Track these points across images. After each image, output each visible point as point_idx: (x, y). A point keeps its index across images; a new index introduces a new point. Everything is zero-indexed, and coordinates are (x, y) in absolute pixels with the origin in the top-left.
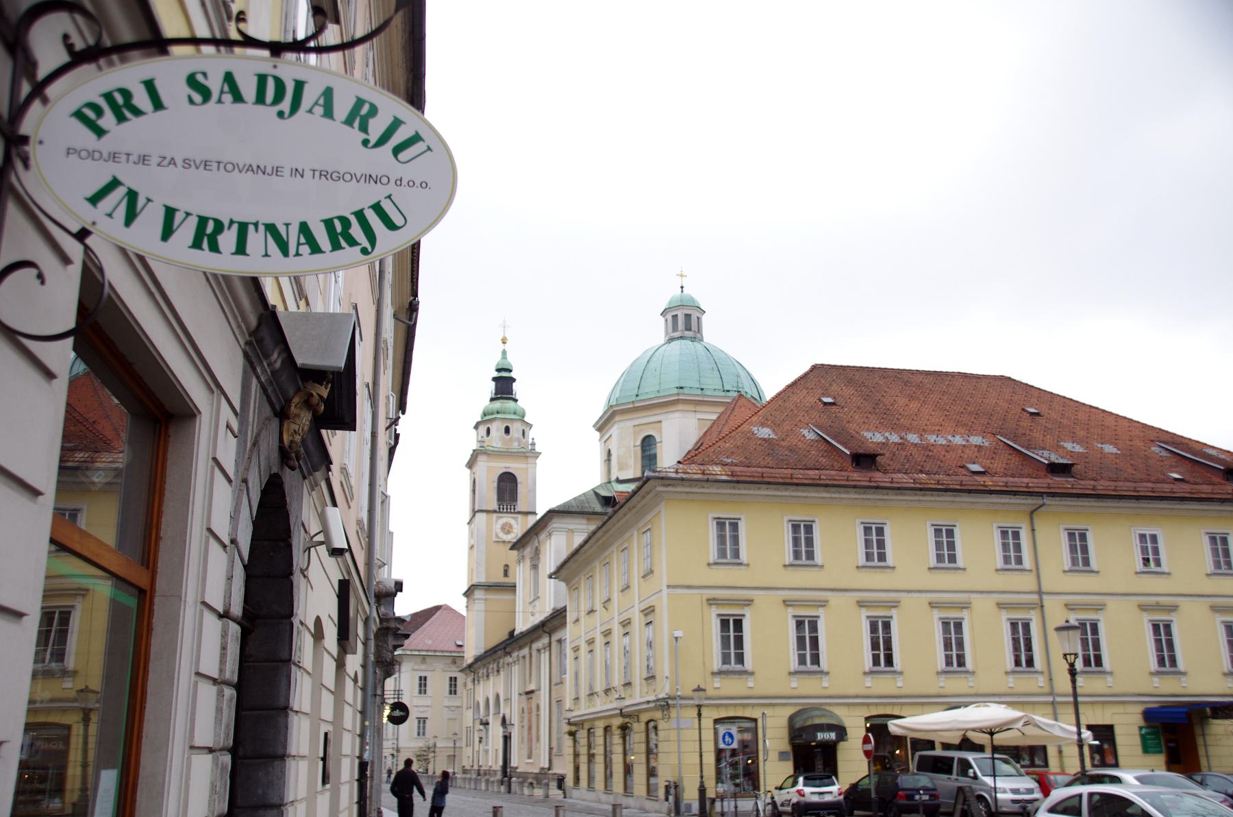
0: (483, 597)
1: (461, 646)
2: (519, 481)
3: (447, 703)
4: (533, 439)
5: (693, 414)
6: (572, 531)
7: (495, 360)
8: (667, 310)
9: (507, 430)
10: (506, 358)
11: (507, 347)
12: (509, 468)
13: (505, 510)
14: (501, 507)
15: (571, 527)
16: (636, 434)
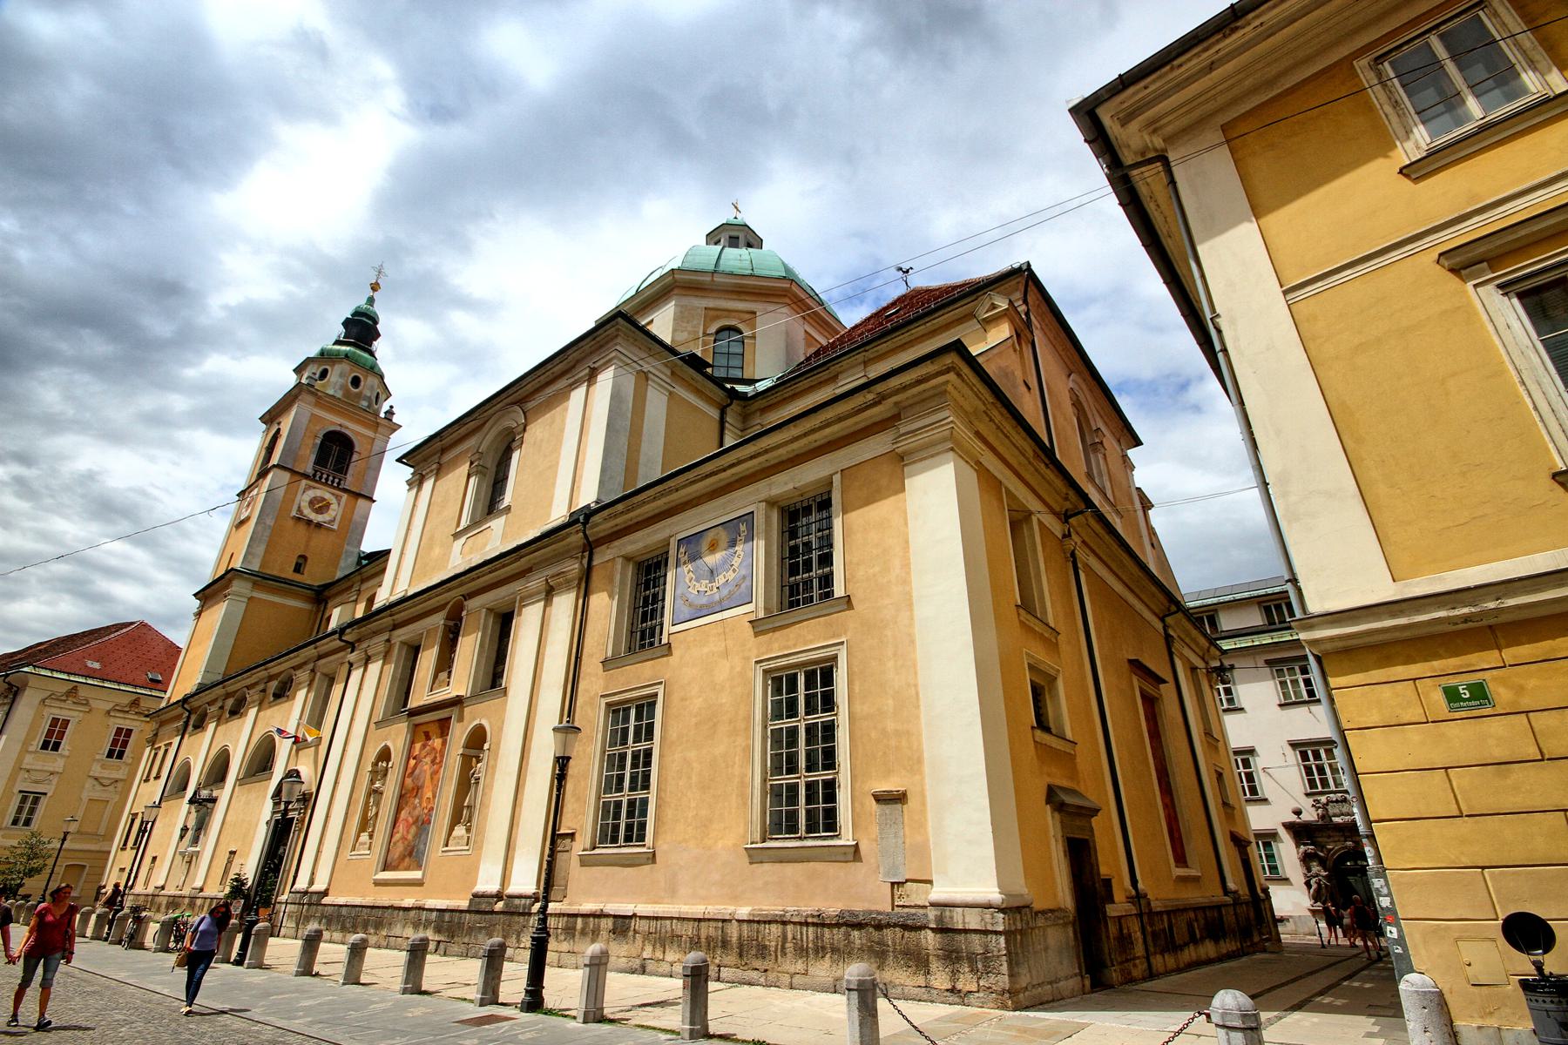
2: (357, 449)
3: (96, 770)
4: (391, 407)
7: (361, 302)
9: (356, 382)
11: (376, 295)
12: (347, 428)
13: (323, 480)
14: (319, 474)
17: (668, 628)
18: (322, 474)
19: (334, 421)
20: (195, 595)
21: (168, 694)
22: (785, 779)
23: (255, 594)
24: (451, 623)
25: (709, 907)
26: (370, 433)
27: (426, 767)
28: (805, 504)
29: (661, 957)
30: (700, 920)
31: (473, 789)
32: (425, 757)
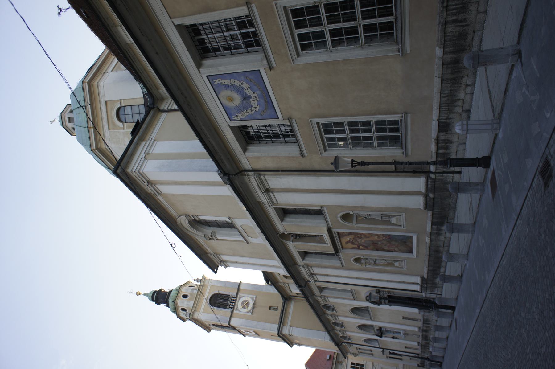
0: (288, 327)
1: (330, 356)
2: (217, 292)
4: (195, 280)
5: (106, 75)
6: (147, 155)
7: (147, 300)
8: (65, 126)
9: (185, 296)
10: (148, 294)
14: (231, 306)
15: (143, 155)
16: (116, 127)
17: (280, 121)
18: (230, 305)
19: (204, 303)
20: (291, 347)
21: (335, 351)
22: (361, 34)
23: (289, 324)
24: (292, 238)
25: (436, 75)
26: (209, 287)
27: (363, 241)
28: (197, 43)
29: (462, 101)
30: (442, 80)
31: (372, 217)
32: (358, 242)
